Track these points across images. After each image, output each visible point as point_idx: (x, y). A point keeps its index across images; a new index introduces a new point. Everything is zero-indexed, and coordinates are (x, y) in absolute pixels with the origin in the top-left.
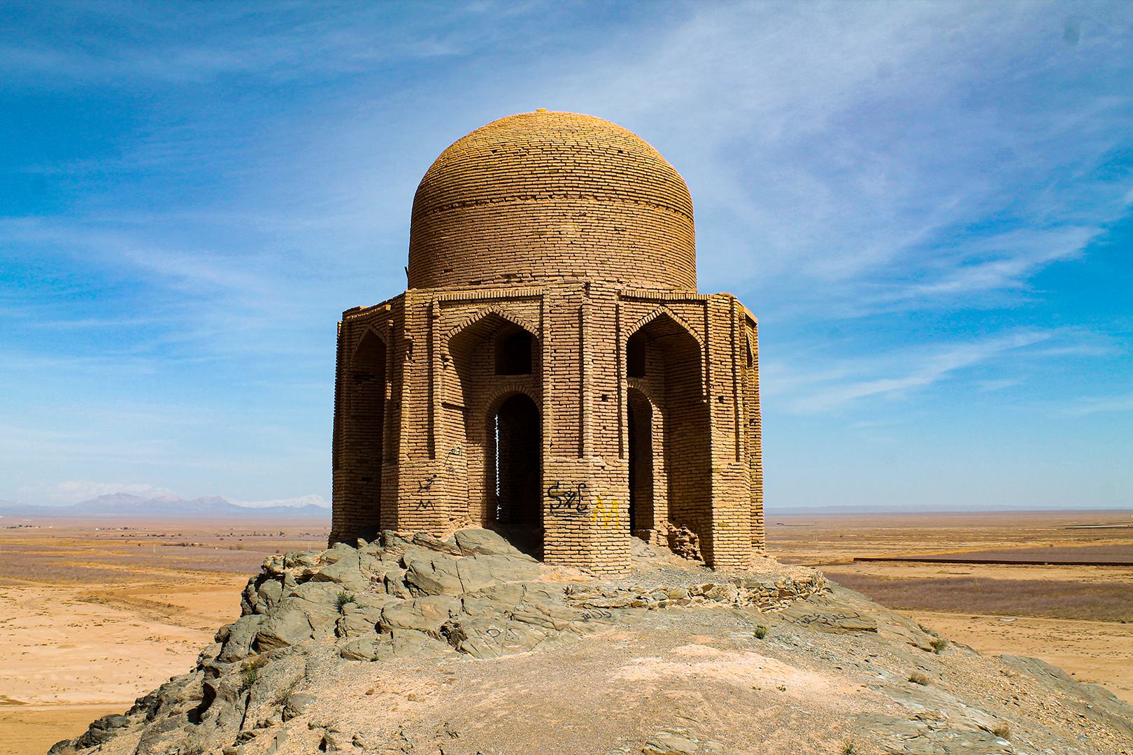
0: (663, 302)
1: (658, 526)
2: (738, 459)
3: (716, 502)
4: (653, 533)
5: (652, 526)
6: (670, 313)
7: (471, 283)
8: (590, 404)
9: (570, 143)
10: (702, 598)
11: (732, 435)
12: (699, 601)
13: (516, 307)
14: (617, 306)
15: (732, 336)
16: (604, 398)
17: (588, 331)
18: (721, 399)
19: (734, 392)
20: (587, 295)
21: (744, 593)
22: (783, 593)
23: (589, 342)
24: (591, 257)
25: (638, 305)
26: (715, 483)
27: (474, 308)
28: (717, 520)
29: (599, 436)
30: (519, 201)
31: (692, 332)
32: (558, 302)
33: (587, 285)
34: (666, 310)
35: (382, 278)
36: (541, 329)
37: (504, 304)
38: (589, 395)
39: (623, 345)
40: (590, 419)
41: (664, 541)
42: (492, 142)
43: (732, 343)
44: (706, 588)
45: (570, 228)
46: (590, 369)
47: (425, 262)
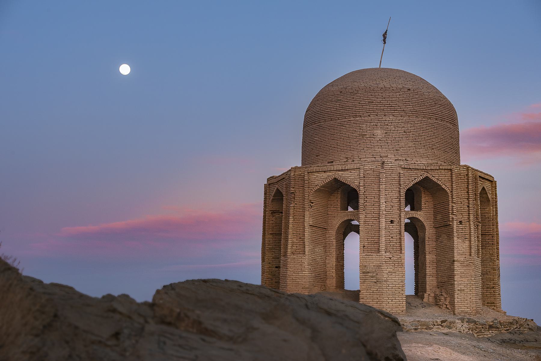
0: (426, 170)
1: (428, 292)
2: (470, 255)
3: (456, 278)
4: (426, 295)
5: (425, 292)
6: (431, 177)
7: (329, 163)
8: (383, 225)
9: (381, 86)
10: (440, 327)
11: (467, 243)
12: (438, 328)
13: (346, 174)
14: (400, 173)
15: (468, 188)
16: (392, 222)
17: (383, 187)
18: (461, 222)
19: (469, 218)
20: (383, 167)
21: (466, 325)
22: (491, 327)
23: (383, 193)
24: (390, 147)
25: (411, 173)
26: (456, 267)
27: (325, 175)
28: (457, 287)
29: (388, 242)
30: (352, 119)
31: (444, 186)
32: (368, 172)
33: (383, 163)
34: (429, 175)
35: (288, 158)
36: (359, 186)
37: (340, 173)
38: (383, 220)
39: (403, 194)
40: (383, 232)
41: (431, 300)
42: (340, 87)
43: (468, 192)
44: (443, 322)
45: (379, 133)
46: (383, 207)
47: (311, 149)
